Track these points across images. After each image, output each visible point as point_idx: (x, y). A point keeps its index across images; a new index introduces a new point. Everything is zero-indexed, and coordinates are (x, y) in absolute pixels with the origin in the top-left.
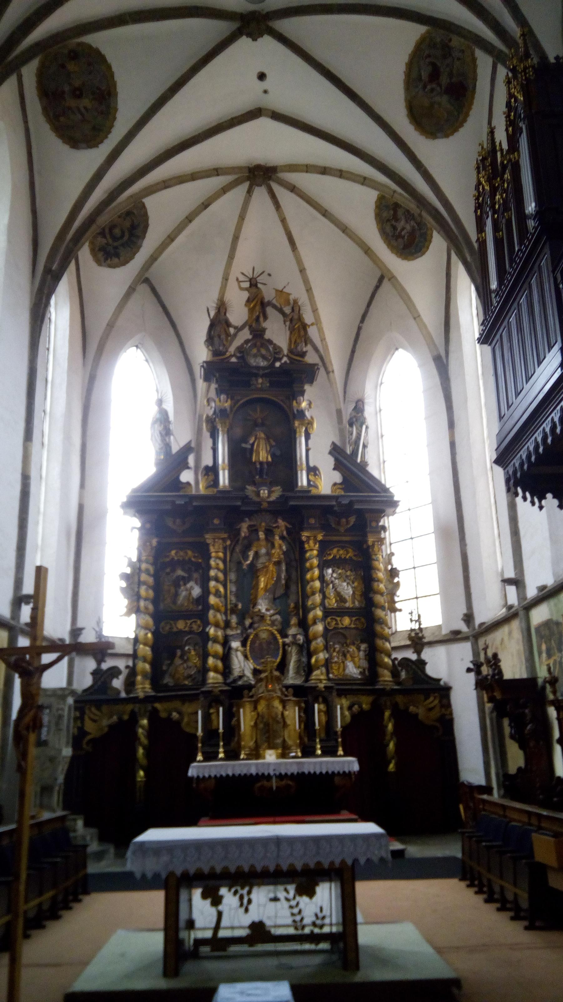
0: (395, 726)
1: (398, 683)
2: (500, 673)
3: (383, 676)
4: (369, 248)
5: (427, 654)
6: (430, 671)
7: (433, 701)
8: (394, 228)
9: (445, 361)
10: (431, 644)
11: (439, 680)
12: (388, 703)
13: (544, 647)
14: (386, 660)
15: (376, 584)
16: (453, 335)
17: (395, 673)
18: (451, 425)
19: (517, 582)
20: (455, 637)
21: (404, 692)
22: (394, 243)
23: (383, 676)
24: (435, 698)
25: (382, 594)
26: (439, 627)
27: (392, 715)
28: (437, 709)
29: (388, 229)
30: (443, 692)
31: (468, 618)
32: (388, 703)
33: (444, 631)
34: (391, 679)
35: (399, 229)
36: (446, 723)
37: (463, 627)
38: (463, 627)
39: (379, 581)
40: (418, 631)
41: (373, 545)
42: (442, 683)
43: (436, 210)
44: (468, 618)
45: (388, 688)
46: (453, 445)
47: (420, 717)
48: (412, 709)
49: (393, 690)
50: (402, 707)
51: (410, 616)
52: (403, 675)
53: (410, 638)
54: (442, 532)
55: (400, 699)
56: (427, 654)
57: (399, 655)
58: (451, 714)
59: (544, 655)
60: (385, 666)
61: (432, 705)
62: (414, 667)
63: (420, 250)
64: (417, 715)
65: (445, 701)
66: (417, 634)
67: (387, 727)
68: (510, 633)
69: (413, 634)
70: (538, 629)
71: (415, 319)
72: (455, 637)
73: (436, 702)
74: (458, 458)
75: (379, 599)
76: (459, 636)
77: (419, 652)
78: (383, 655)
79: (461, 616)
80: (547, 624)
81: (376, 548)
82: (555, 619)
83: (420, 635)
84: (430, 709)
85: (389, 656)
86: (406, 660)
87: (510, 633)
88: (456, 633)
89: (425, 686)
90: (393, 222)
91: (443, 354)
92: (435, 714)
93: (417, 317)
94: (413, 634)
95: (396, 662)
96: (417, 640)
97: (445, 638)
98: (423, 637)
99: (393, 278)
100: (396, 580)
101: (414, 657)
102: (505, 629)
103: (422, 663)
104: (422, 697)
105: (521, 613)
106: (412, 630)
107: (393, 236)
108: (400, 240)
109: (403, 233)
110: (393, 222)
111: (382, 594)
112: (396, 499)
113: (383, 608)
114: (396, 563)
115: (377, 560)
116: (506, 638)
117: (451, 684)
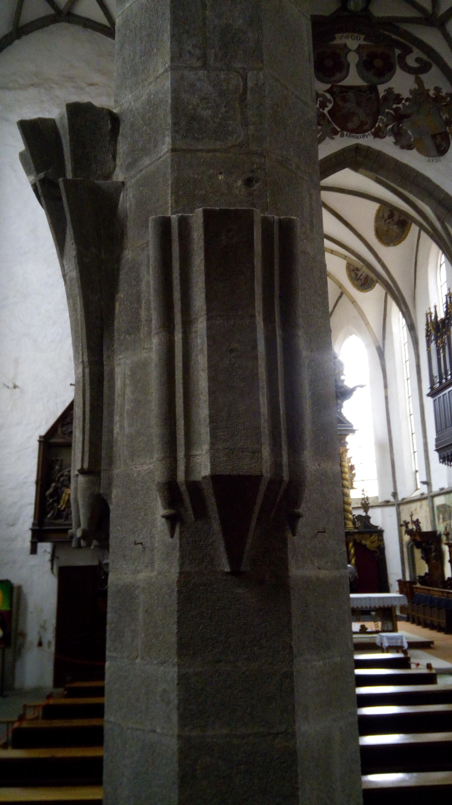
0: (355, 551)
1: (356, 528)
2: (420, 528)
3: (348, 525)
4: (342, 285)
5: (371, 513)
6: (373, 522)
7: (374, 537)
8: (357, 274)
9: (382, 350)
10: (372, 507)
11: (377, 527)
12: (351, 539)
13: (441, 516)
14: (350, 516)
15: (344, 475)
16: (387, 336)
17: (354, 523)
18: (386, 386)
19: (428, 483)
20: (387, 504)
21: (358, 533)
22: (356, 282)
23: (348, 525)
24: (375, 536)
25: (347, 480)
26: (377, 498)
27: (354, 545)
28: (376, 542)
29: (353, 275)
30: (379, 533)
31: (395, 495)
32: (351, 539)
33: (380, 500)
34: (352, 526)
35: (359, 275)
36: (381, 549)
37: (392, 499)
38: (392, 499)
39: (345, 473)
40: (366, 500)
41: (343, 454)
42: (379, 528)
43: (387, 282)
44: (395, 495)
45: (352, 531)
46: (386, 398)
47: (368, 546)
48: (363, 542)
49: (355, 532)
50: (358, 541)
51: (362, 492)
52: (358, 524)
53: (362, 504)
54: (380, 446)
55: (357, 537)
56: (371, 513)
57: (357, 513)
58: (383, 544)
59: (441, 520)
60: (349, 519)
61: (374, 540)
62: (364, 520)
63: (370, 287)
64: (365, 546)
65: (380, 538)
66: (365, 502)
67: (350, 551)
68: (421, 506)
69: (363, 502)
70: (438, 507)
71: (366, 325)
72: (387, 504)
73: (376, 538)
74: (390, 406)
75: (346, 483)
76: (389, 504)
77: (366, 511)
78: (348, 514)
79: (391, 493)
80: (444, 506)
81: (344, 455)
82: (448, 504)
83: (367, 502)
84: (373, 542)
85: (351, 514)
86: (360, 516)
87: (421, 506)
88: (388, 502)
89: (371, 530)
90: (356, 272)
91: (382, 346)
92: (376, 544)
93: (367, 324)
94: (363, 502)
95: (355, 517)
96: (365, 505)
97: (381, 504)
98: (368, 504)
99: (353, 302)
100: (353, 472)
101: (364, 514)
102: (418, 504)
103: (368, 518)
104: (369, 536)
105: (430, 498)
106: (363, 499)
107: (355, 279)
108: (359, 281)
109: (361, 277)
110: (356, 272)
111: (347, 480)
112: (354, 428)
113: (348, 488)
114: (353, 462)
115: (345, 461)
116: (418, 509)
117: (384, 528)
